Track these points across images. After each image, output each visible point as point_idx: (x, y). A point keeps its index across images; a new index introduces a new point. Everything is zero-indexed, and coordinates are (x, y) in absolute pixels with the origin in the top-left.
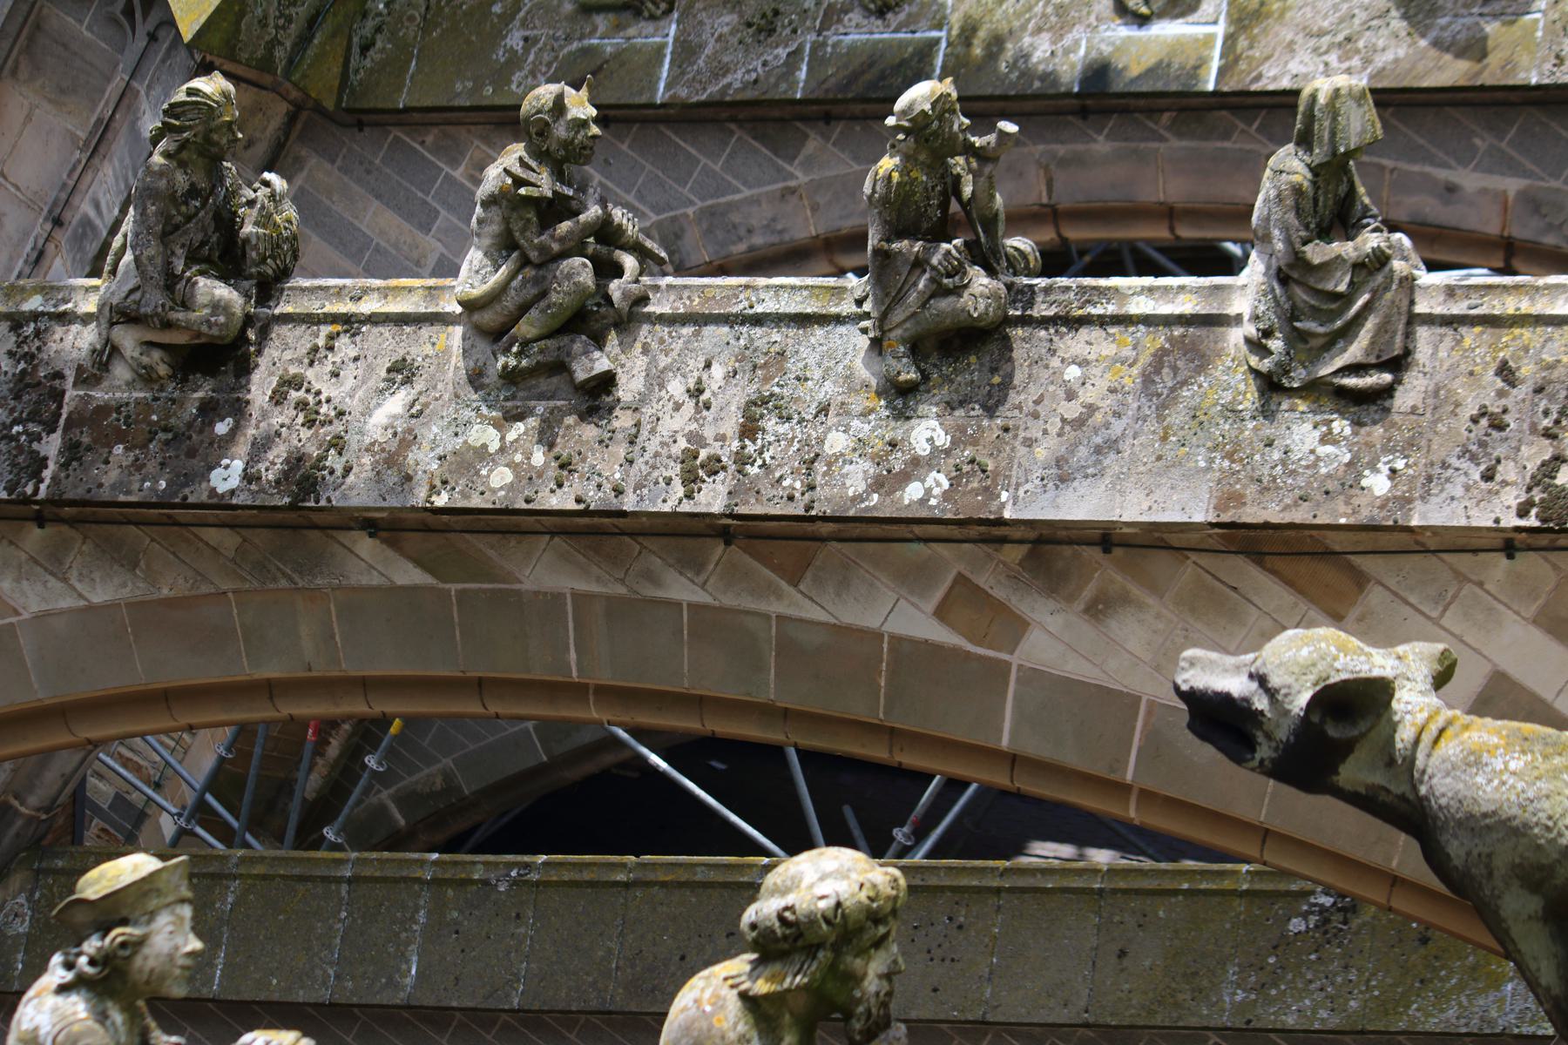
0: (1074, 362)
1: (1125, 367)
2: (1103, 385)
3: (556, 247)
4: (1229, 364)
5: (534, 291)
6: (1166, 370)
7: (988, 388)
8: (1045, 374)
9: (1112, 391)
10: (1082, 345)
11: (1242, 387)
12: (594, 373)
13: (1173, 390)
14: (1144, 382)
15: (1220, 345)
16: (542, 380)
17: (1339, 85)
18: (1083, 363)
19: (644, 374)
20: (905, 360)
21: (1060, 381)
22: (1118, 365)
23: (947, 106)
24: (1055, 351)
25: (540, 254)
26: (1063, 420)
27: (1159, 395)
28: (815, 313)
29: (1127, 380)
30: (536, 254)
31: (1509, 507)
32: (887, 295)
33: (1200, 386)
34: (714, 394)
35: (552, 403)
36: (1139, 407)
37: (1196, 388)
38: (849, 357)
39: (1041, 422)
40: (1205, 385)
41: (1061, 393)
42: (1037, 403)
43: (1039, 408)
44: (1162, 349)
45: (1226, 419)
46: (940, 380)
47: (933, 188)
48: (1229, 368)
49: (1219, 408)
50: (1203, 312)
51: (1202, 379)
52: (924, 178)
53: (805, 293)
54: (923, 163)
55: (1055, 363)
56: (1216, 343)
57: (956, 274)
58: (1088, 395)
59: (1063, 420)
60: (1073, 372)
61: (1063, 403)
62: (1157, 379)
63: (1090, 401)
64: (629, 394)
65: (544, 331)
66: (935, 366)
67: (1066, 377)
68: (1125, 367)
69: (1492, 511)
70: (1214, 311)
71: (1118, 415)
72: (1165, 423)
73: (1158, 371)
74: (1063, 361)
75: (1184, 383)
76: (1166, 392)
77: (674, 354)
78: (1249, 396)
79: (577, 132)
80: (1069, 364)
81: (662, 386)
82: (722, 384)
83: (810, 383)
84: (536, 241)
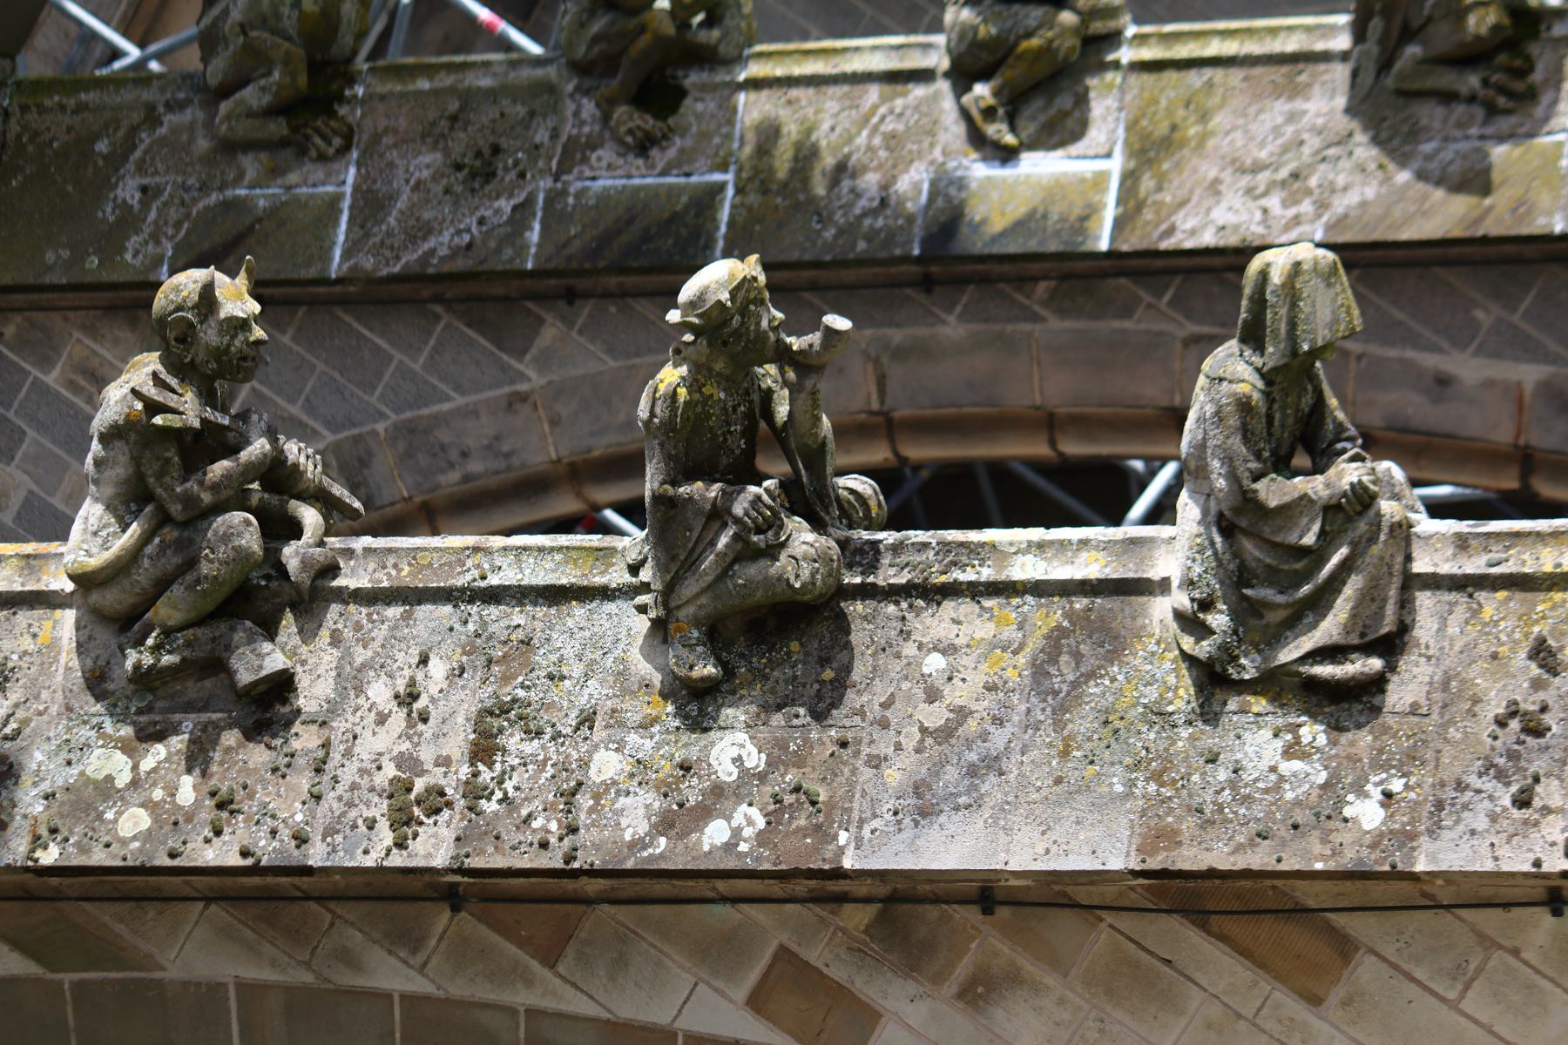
0: (935, 649)
1: (1008, 655)
2: (977, 679)
3: (207, 498)
4: (1152, 647)
5: (177, 560)
6: (1064, 658)
7: (816, 686)
8: (896, 666)
9: (991, 688)
10: (947, 624)
11: (1172, 680)
12: (264, 673)
13: (1075, 685)
14: (1034, 674)
15: (1139, 622)
16: (190, 684)
17: (1299, 258)
18: (949, 650)
19: (333, 673)
20: (700, 649)
21: (917, 675)
22: (998, 651)
23: (752, 295)
24: (909, 633)
25: (185, 509)
26: (924, 730)
27: (1056, 693)
28: (572, 585)
29: (1011, 674)
30: (179, 507)
31: (1553, 844)
32: (673, 558)
33: (1113, 680)
34: (433, 700)
35: (204, 717)
36: (1029, 711)
37: (1107, 682)
38: (621, 646)
39: (892, 733)
40: (1120, 677)
41: (919, 692)
42: (885, 706)
43: (888, 713)
44: (1059, 628)
45: (1152, 724)
46: (750, 677)
47: (734, 409)
48: (1153, 654)
49: (1141, 710)
50: (1115, 576)
51: (1116, 669)
52: (722, 395)
53: (558, 557)
54: (719, 374)
55: (910, 649)
56: (1134, 618)
57: (770, 528)
58: (957, 694)
59: (924, 730)
60: (935, 663)
61: (922, 705)
62: (1053, 671)
63: (960, 702)
64: (313, 702)
65: (193, 615)
66: (742, 656)
67: (926, 670)
68: (1008, 655)
69: (1530, 850)
70: (1131, 575)
71: (999, 721)
72: (1066, 732)
73: (1053, 660)
74: (920, 647)
75: (1091, 675)
76: (1065, 688)
77: (376, 645)
78: (1181, 692)
79: (233, 337)
80: (929, 651)
81: (359, 690)
82: (445, 686)
83: (567, 682)
84: (178, 490)
